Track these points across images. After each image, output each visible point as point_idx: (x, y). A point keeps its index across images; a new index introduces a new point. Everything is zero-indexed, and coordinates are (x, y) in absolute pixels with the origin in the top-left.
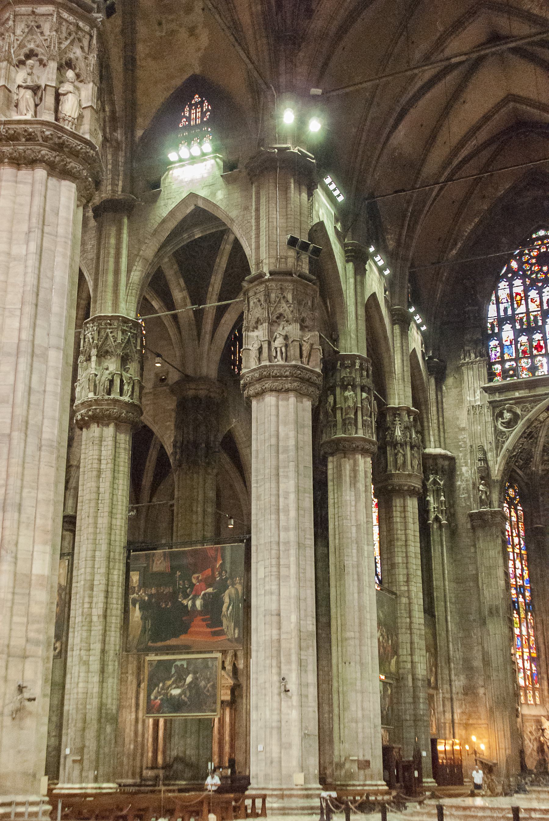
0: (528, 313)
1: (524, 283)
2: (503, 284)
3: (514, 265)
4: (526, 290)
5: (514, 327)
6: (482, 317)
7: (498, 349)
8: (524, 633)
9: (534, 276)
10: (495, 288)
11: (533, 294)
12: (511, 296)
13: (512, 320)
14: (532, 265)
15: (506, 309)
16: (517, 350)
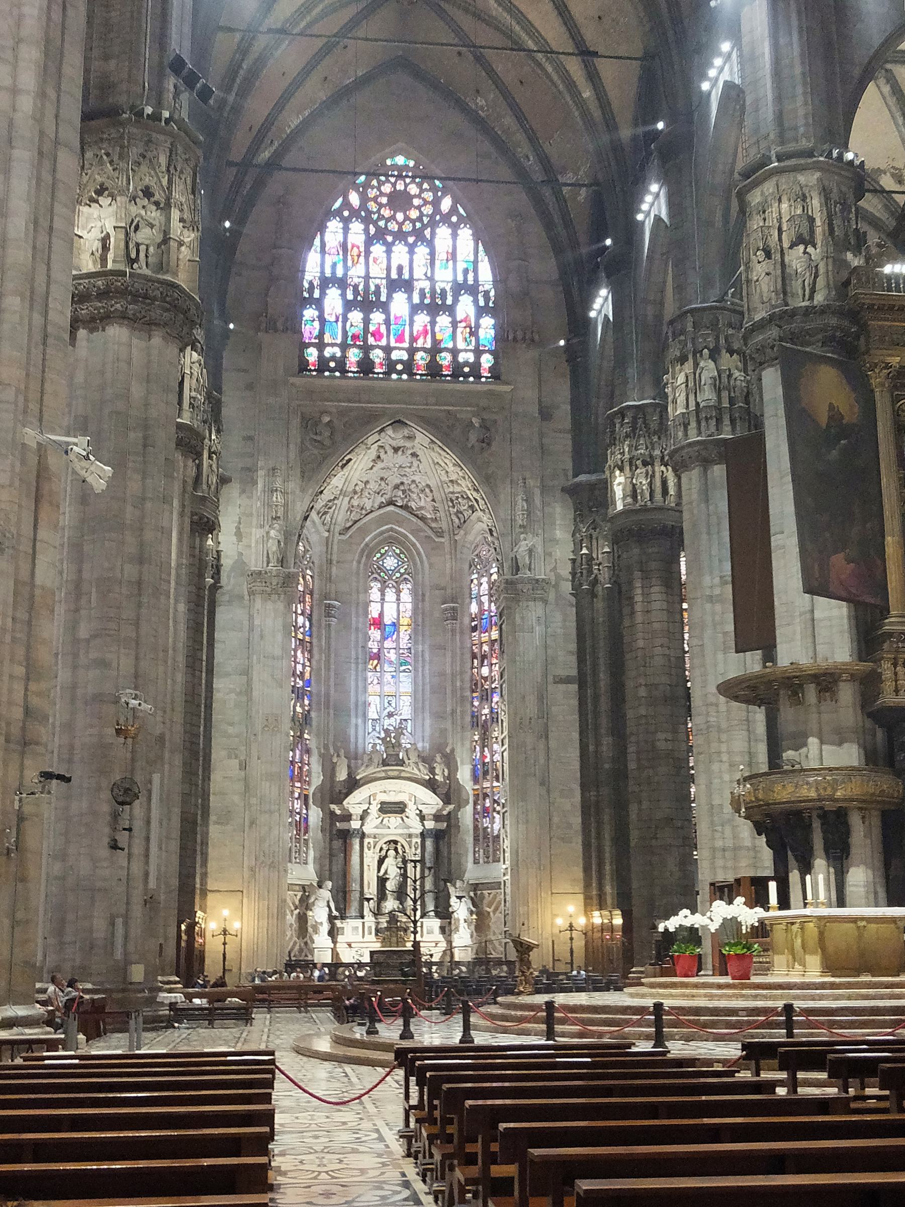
0: (367, 278)
1: (366, 231)
2: (334, 226)
3: (354, 199)
4: (369, 242)
5: (343, 295)
6: (298, 270)
7: (317, 324)
8: (297, 759)
9: (382, 223)
10: (322, 228)
11: (378, 250)
12: (344, 246)
13: (342, 283)
14: (381, 206)
15: (334, 265)
16: (345, 332)
